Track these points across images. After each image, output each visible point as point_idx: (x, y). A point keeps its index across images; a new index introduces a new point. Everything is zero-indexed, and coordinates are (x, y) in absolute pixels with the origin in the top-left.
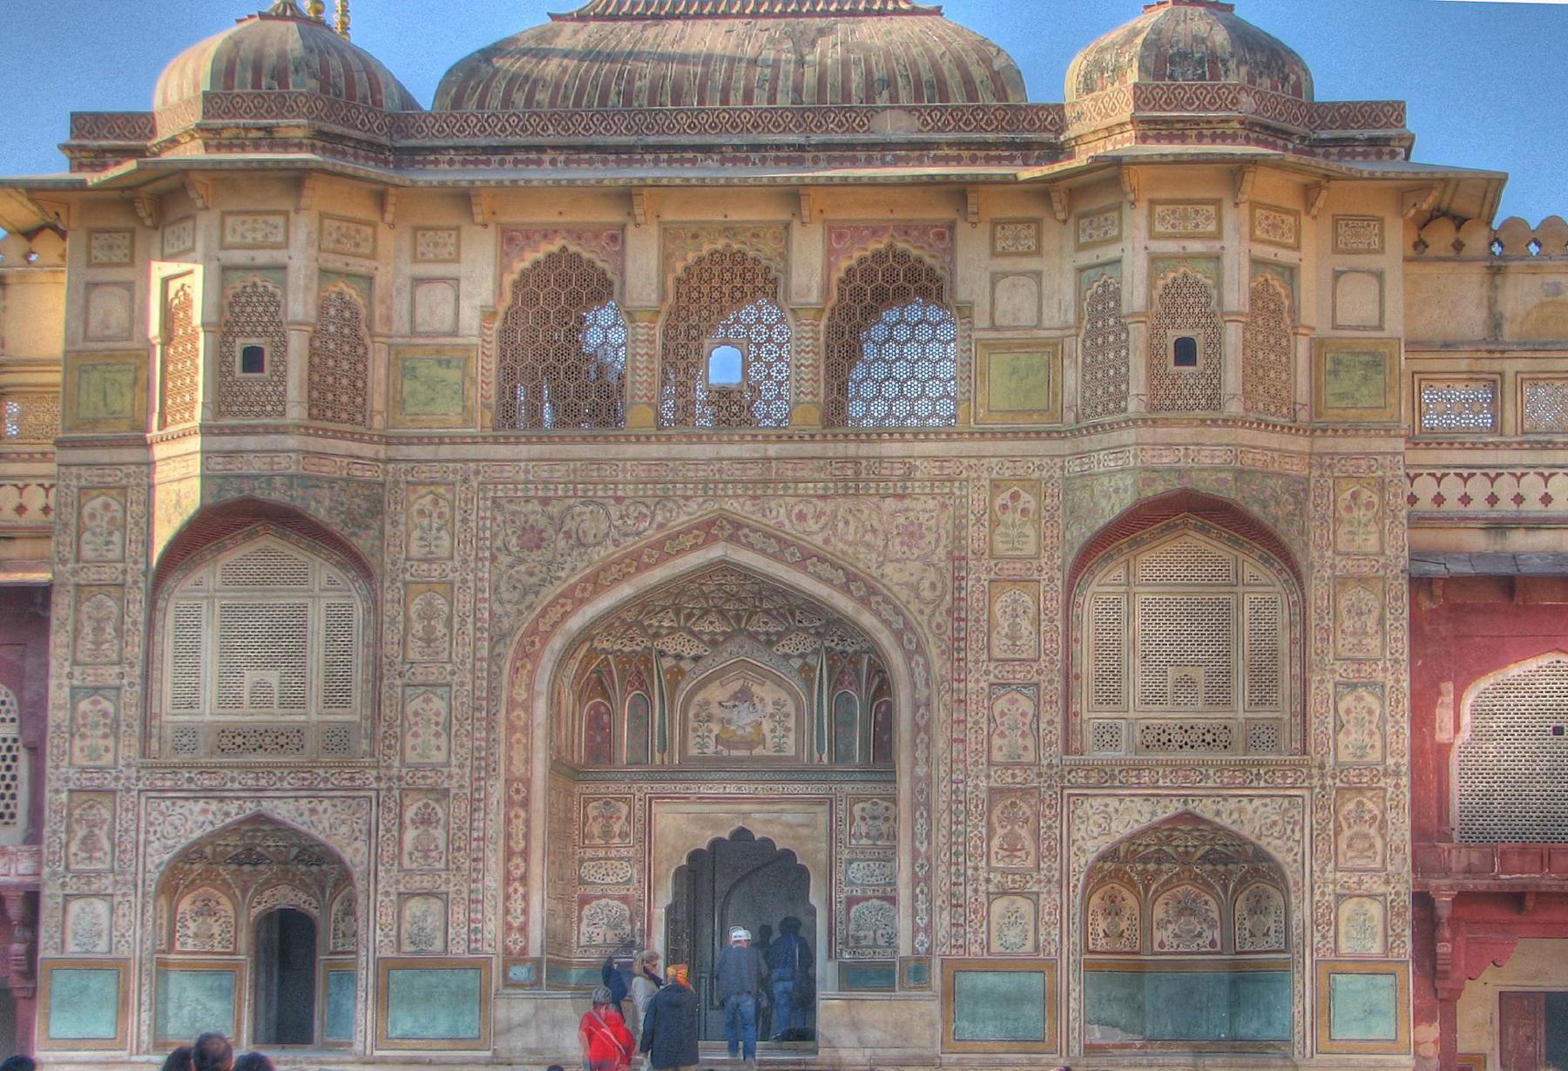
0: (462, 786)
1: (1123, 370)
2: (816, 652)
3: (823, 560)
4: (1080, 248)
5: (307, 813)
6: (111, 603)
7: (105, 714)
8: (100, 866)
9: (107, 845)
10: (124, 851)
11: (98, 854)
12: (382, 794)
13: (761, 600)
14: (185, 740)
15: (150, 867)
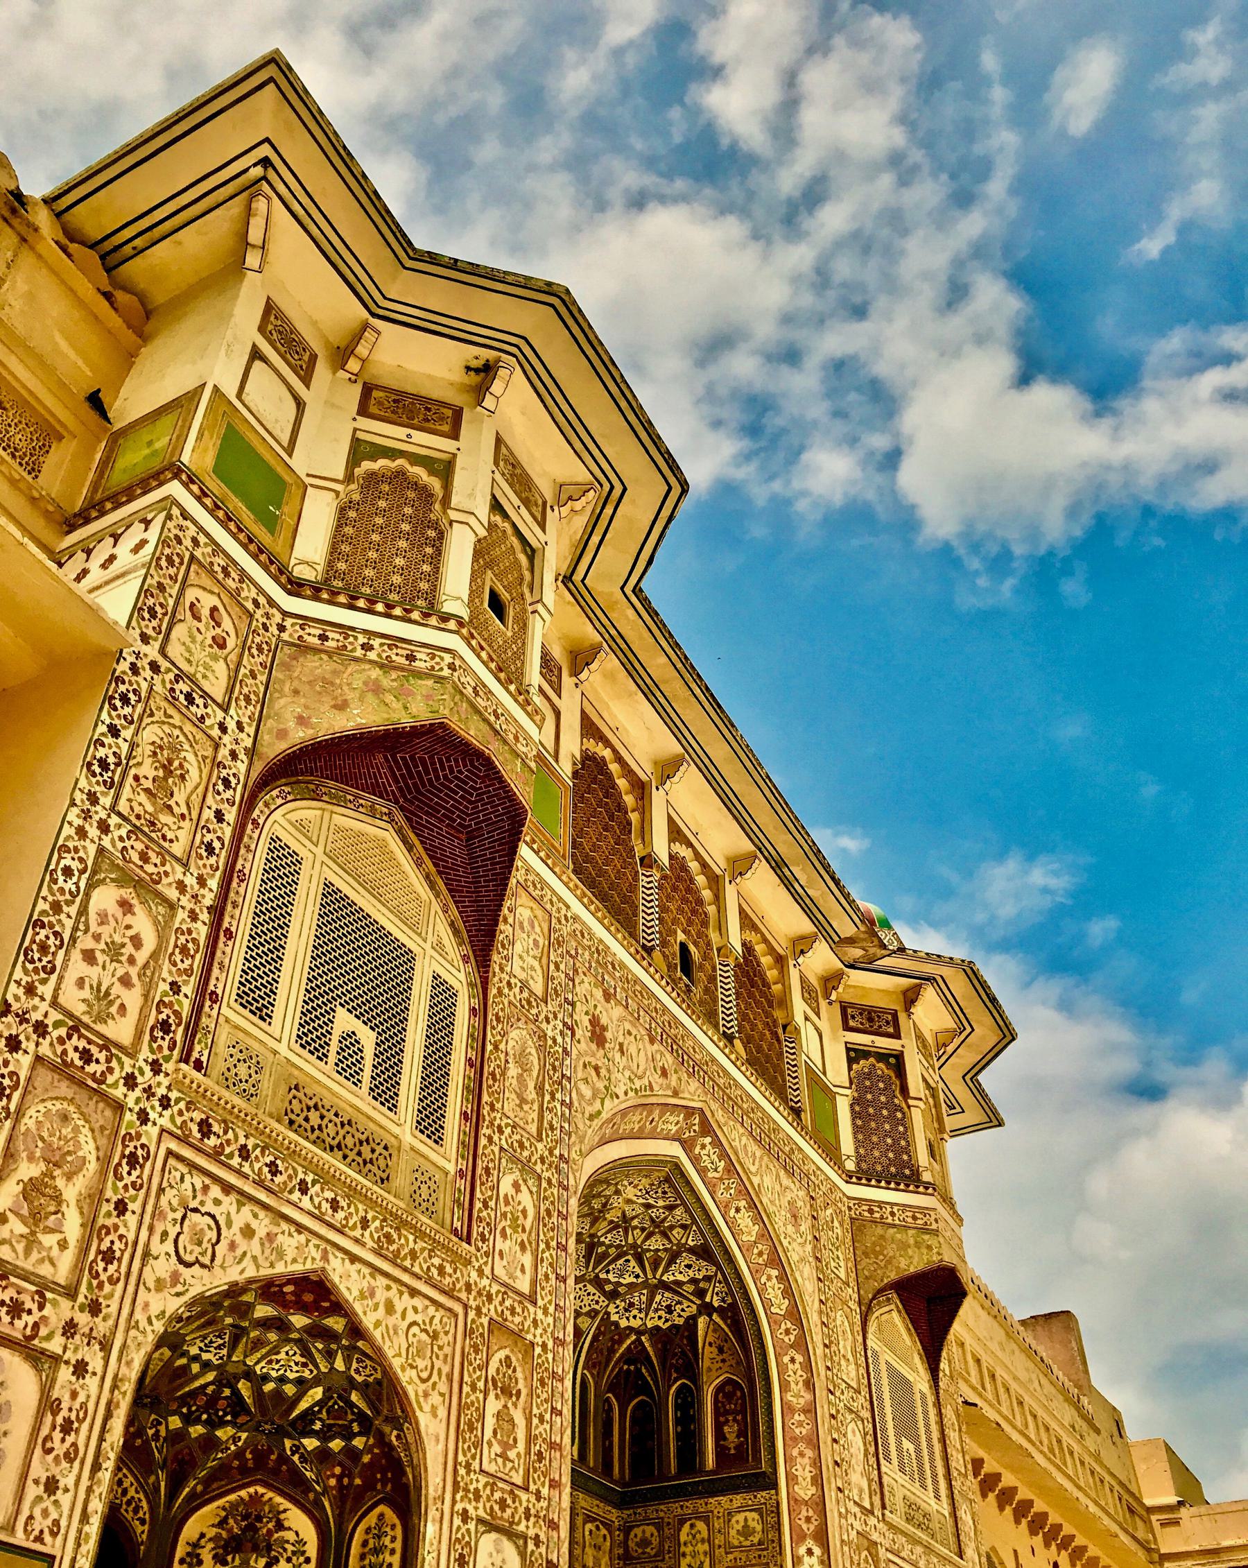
0: (544, 1346)
1: (903, 1143)
2: (592, 1314)
3: (752, 1205)
4: (847, 1028)
5: (381, 1309)
6: (190, 757)
7: (137, 941)
8: (45, 1270)
9: (73, 1225)
10: (108, 1256)
11: (49, 1240)
12: (472, 1314)
13: (609, 1231)
14: (242, 1070)
15: (139, 1316)
